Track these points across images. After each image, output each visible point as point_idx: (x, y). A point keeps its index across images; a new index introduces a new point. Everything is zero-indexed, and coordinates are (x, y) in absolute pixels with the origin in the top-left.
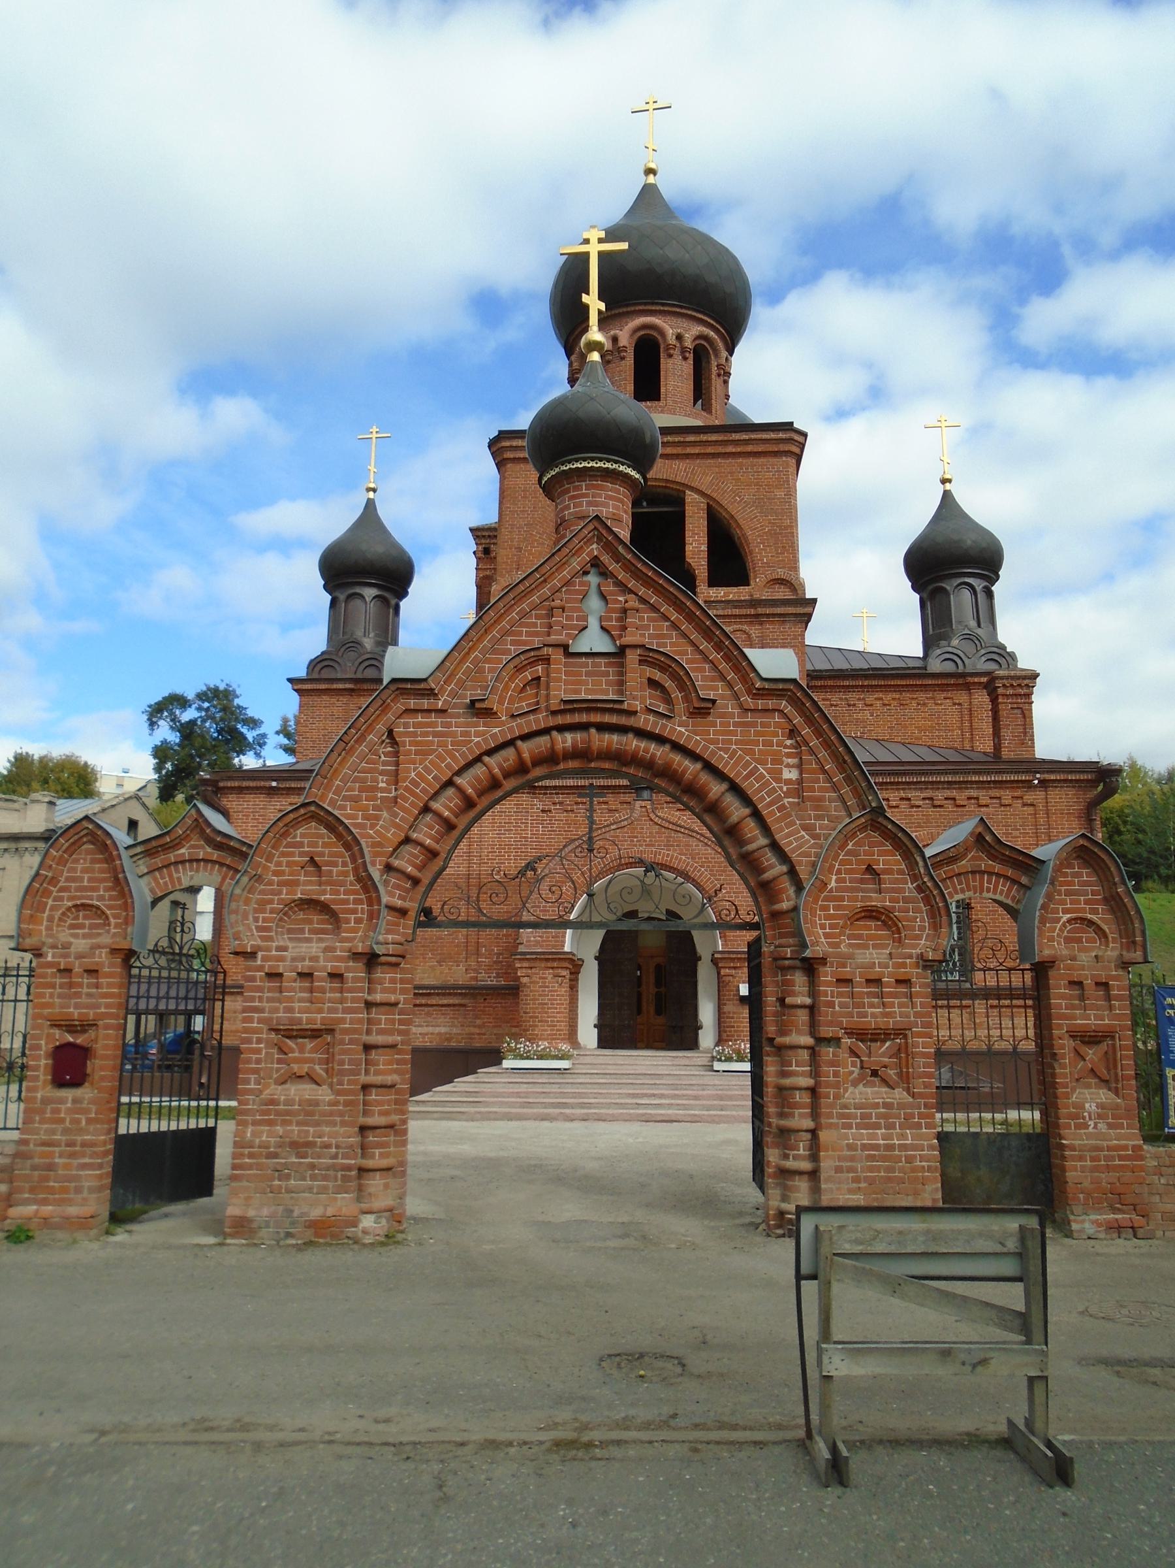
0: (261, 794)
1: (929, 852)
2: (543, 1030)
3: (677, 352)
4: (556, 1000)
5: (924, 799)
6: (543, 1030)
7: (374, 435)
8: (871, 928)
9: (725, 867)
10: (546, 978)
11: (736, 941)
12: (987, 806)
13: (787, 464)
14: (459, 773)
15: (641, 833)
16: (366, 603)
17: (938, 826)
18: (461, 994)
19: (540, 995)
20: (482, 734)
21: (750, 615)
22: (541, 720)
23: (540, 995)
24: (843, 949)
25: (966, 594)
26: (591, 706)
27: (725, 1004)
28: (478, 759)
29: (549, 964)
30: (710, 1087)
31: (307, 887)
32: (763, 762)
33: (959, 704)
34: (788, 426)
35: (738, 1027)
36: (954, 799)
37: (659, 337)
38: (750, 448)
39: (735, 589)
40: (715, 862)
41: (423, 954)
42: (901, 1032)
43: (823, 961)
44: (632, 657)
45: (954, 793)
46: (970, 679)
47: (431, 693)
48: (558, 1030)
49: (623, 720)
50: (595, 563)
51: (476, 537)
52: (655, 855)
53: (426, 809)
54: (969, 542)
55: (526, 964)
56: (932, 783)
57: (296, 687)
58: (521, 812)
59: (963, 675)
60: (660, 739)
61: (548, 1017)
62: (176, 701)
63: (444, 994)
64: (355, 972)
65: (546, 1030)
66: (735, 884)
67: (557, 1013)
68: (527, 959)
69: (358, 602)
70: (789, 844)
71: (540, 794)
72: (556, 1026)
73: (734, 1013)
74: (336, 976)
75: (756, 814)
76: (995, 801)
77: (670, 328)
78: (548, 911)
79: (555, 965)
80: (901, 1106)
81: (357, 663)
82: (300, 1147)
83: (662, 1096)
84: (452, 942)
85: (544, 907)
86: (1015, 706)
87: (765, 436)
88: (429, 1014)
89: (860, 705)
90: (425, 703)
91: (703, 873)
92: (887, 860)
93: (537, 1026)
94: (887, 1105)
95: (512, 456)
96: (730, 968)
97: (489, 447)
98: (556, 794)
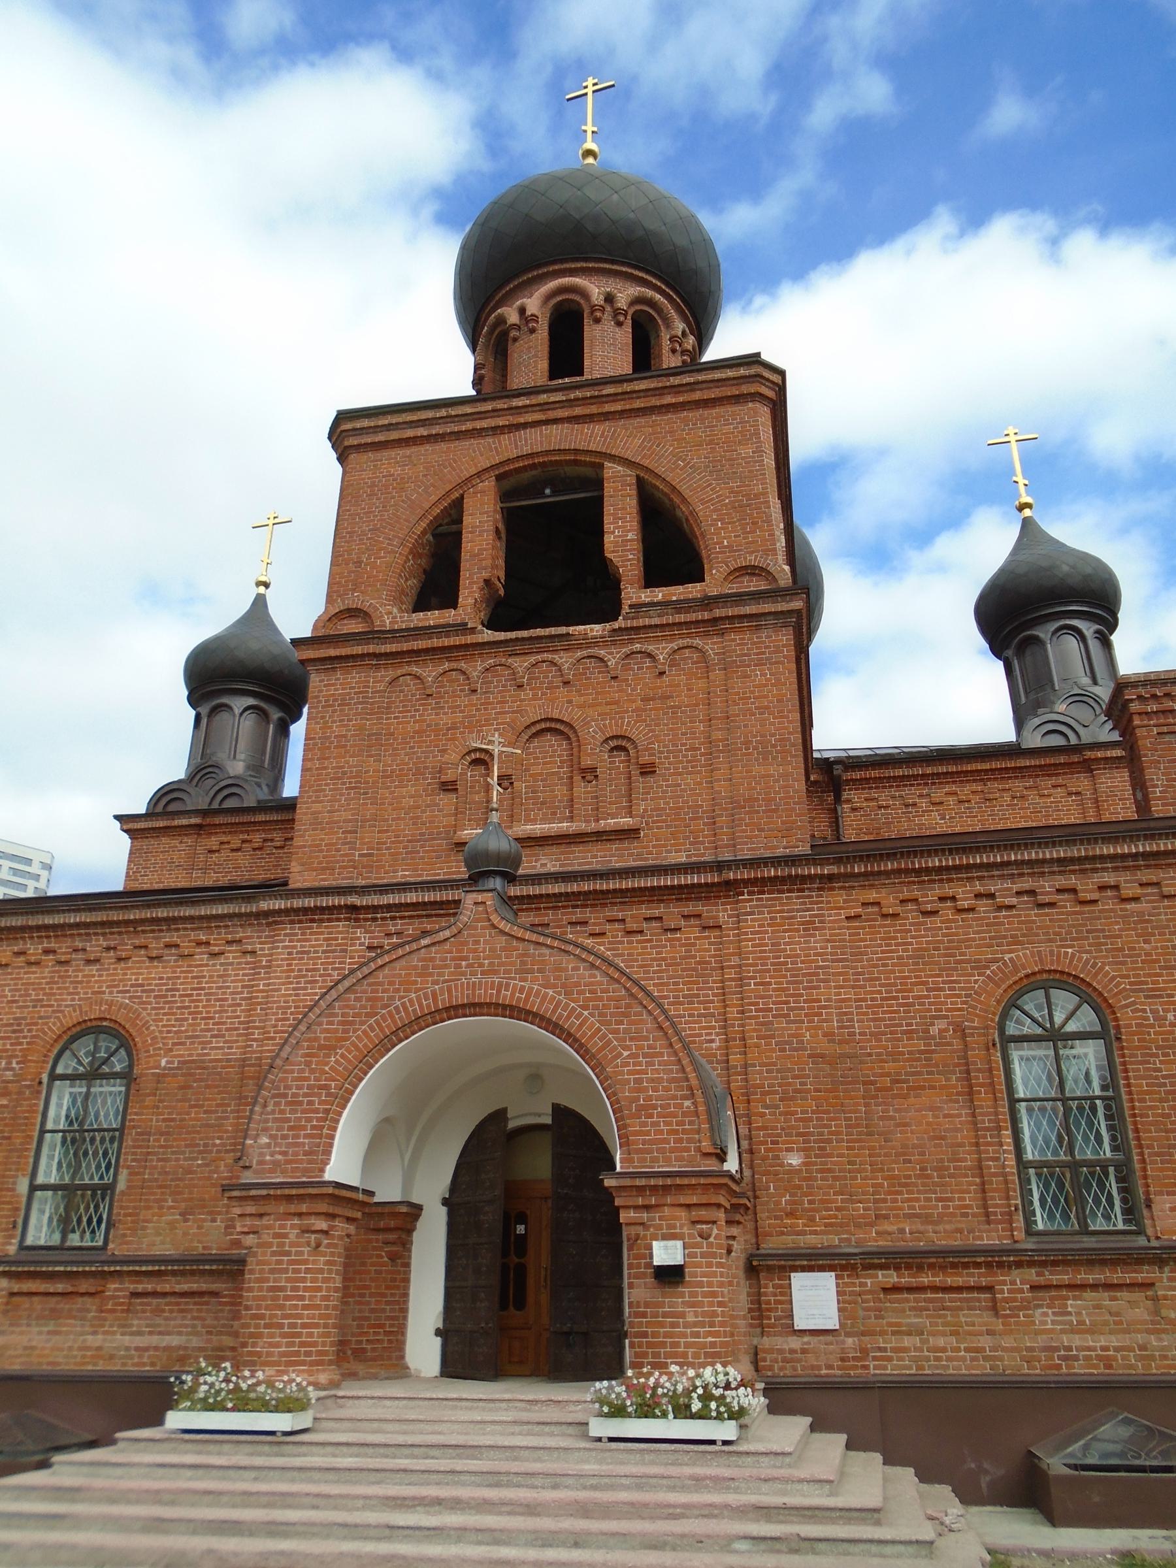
2: (271, 1345)
3: (607, 316)
4: (304, 1280)
5: (1018, 893)
6: (271, 1345)
9: (628, 1006)
10: (285, 1236)
11: (650, 1151)
12: (1136, 899)
13: (756, 413)
15: (475, 951)
16: (234, 715)
17: (1050, 941)
18: (211, 1272)
19: (272, 1271)
21: (703, 621)
23: (272, 1271)
25: (1072, 643)
29: (293, 1208)
30: (570, 1481)
33: (1078, 793)
34: (754, 359)
35: (655, 1335)
36: (1074, 891)
37: (582, 302)
38: (697, 396)
39: (680, 589)
40: (610, 999)
41: (156, 1201)
45: (1073, 881)
46: (1089, 754)
48: (302, 1344)
52: (499, 992)
54: (1065, 568)
55: (250, 1209)
56: (1030, 863)
57: (125, 827)
58: (334, 951)
59: (1078, 749)
61: (285, 1317)
63: (183, 1273)
65: (277, 1345)
66: (647, 1039)
67: (305, 1307)
68: (253, 1198)
69: (224, 716)
71: (366, 920)
72: (299, 1335)
73: (647, 1305)
76: (1149, 890)
77: (595, 289)
78: (301, 1103)
79: (304, 1208)
81: (212, 793)
83: (456, 1504)
84: (209, 1178)
85: (294, 1095)
86: (1165, 729)
87: (718, 375)
88: (158, 1311)
89: (923, 804)
91: (586, 1019)
93: (260, 1336)
95: (356, 443)
96: (636, 1208)
98: (393, 918)
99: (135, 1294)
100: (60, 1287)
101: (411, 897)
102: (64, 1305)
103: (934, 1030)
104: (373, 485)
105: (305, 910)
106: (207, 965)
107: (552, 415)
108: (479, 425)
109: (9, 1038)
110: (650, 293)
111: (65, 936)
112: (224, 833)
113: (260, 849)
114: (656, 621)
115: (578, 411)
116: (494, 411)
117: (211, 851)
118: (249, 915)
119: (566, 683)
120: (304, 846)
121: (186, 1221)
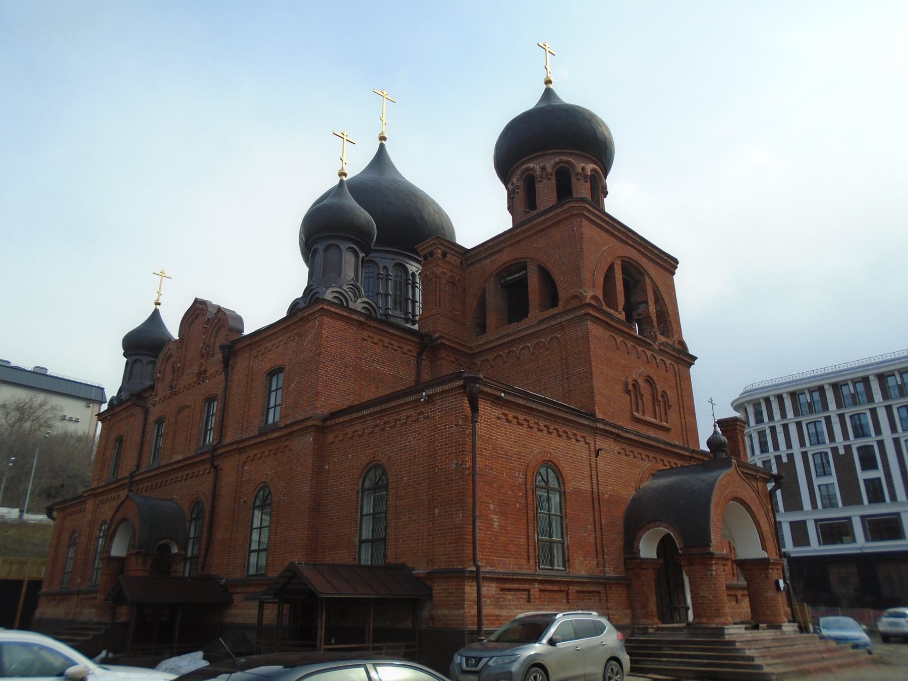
0: (489, 400)
27: (767, 592)
99: (578, 592)
100: (556, 588)
101: (633, 437)
102: (555, 596)
105: (607, 431)
106: (575, 445)
109: (517, 461)
111: (532, 414)
112: (371, 331)
113: (386, 347)
114: (669, 351)
115: (641, 249)
116: (623, 232)
117: (364, 339)
118: (592, 428)
119: (648, 363)
120: (598, 401)
121: (585, 560)
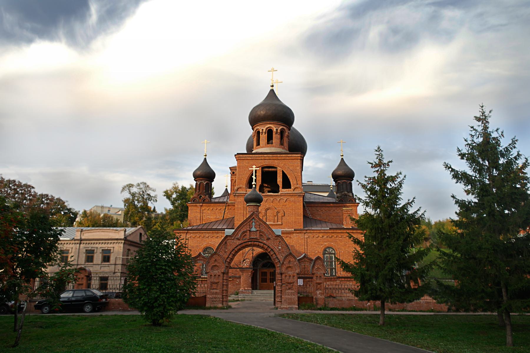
1: (298, 259)
7: (206, 142)
8: (290, 269)
14: (235, 248)
20: (238, 242)
22: (246, 240)
24: (286, 272)
26: (253, 239)
28: (238, 246)
31: (216, 264)
32: (276, 246)
38: (291, 158)
42: (293, 283)
43: (283, 273)
44: (258, 232)
47: (232, 237)
49: (257, 240)
50: (254, 218)
51: (231, 170)
53: (231, 253)
60: (262, 243)
62: (130, 186)
64: (222, 275)
70: (279, 257)
74: (219, 275)
75: (275, 253)
80: (293, 293)
82: (215, 298)
90: (231, 238)
92: (292, 259)
94: (291, 293)
97: (235, 155)
103: (316, 252)
104: (243, 166)
107: (270, 158)
108: (259, 158)
110: (283, 127)
115: (274, 158)
